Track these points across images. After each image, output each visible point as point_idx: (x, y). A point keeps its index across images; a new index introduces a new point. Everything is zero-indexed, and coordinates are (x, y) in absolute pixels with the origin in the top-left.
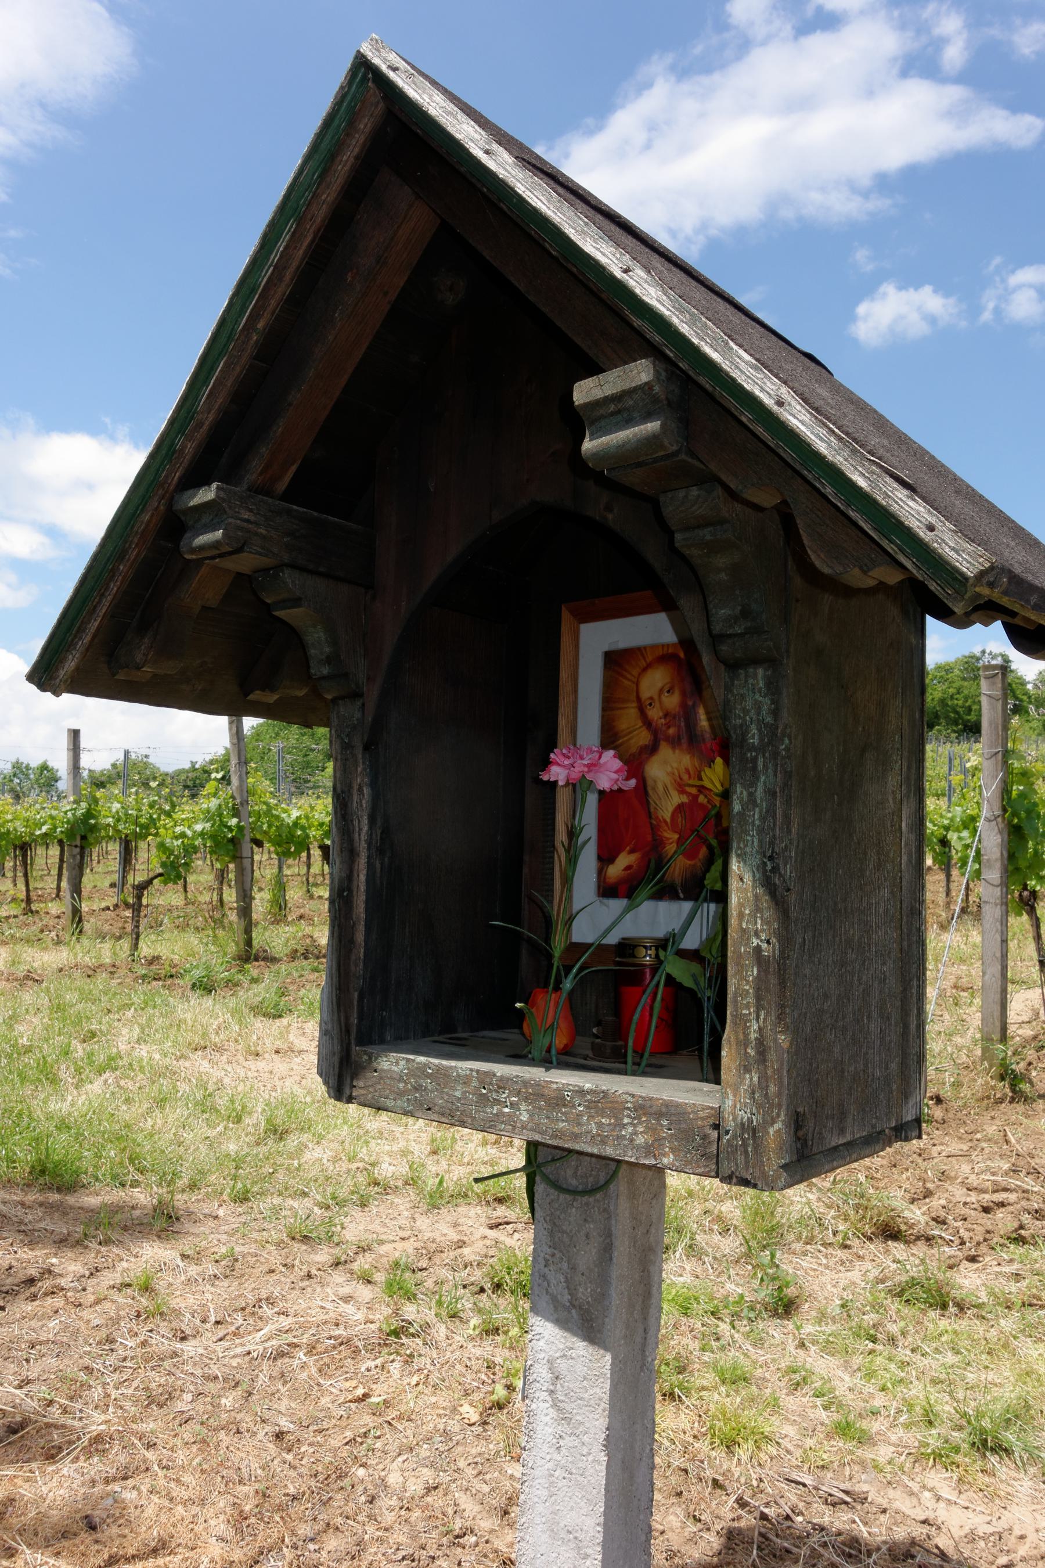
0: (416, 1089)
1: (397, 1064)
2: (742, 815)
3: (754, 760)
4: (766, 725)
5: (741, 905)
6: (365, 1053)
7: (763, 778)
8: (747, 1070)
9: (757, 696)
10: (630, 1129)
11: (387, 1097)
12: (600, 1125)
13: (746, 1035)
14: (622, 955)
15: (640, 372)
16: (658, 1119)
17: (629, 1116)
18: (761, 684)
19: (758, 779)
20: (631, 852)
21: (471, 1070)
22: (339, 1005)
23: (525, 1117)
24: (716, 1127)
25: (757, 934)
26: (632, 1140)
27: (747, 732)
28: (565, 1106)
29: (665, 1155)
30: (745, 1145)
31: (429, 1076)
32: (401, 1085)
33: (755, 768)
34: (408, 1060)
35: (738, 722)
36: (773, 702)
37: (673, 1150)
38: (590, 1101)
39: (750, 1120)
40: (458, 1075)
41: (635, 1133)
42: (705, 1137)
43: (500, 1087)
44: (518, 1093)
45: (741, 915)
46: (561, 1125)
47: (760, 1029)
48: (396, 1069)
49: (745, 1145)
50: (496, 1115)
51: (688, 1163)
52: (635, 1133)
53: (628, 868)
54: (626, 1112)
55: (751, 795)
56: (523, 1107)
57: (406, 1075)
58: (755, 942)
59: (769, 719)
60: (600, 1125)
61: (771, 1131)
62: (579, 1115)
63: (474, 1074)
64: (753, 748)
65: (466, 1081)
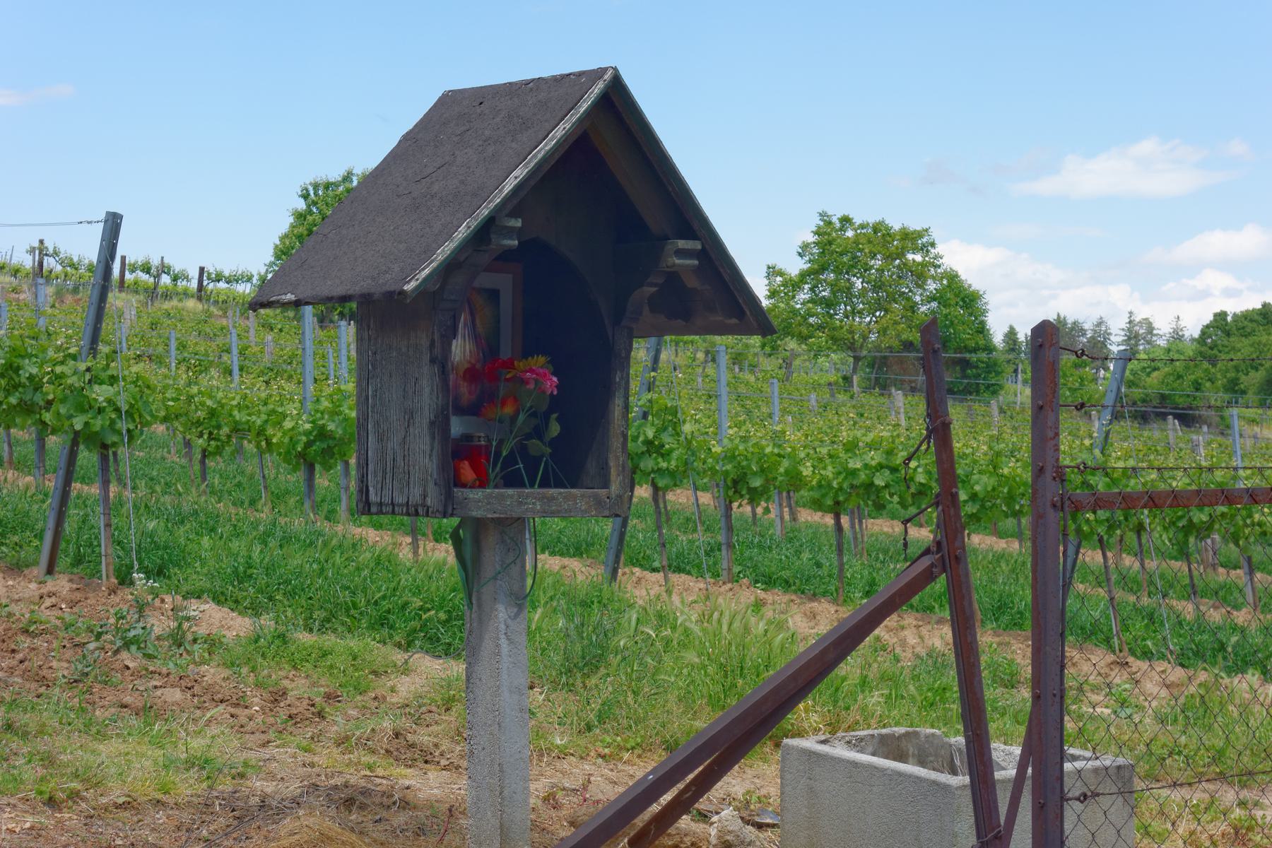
15: (697, 245)
65: (512, 497)
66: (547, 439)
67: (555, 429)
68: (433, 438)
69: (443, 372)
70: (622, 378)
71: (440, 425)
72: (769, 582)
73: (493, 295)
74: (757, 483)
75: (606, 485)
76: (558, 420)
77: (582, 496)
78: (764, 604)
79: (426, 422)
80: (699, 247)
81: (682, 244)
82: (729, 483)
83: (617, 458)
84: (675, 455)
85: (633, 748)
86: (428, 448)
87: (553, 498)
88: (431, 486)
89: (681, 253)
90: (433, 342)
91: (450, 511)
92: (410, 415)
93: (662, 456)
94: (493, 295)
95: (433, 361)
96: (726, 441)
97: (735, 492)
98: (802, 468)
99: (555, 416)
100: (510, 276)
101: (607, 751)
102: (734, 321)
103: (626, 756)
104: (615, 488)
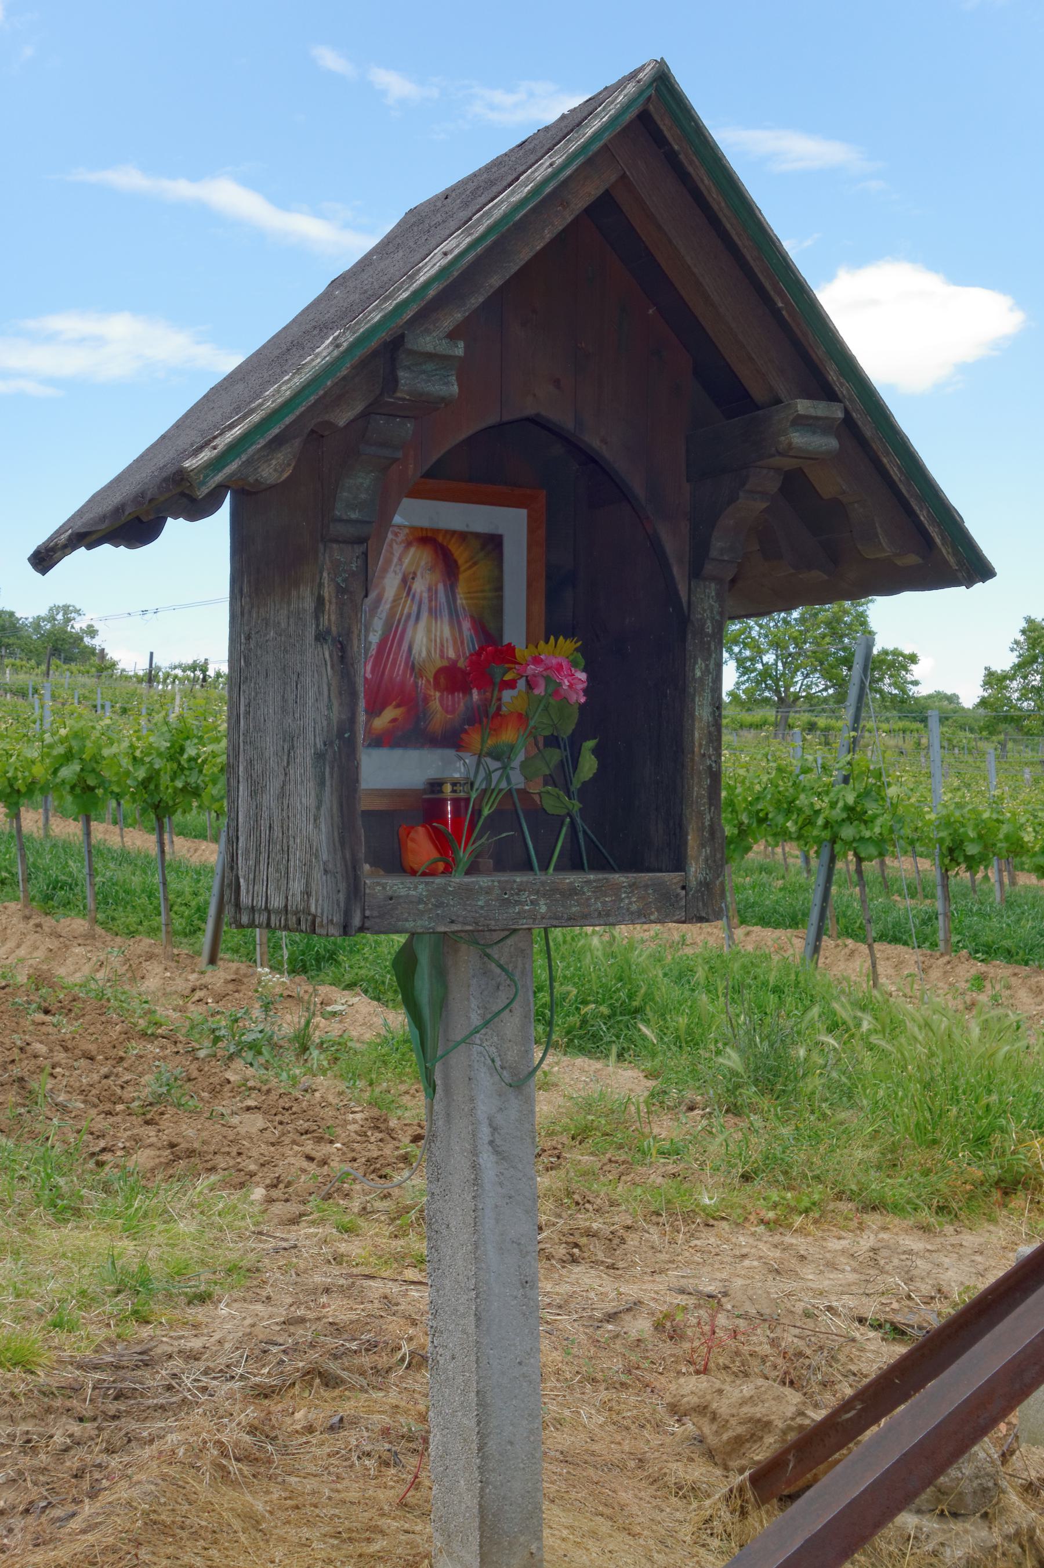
0: (437, 907)
1: (416, 888)
2: (701, 679)
3: (709, 643)
4: (717, 621)
5: (701, 739)
6: (378, 884)
7: (714, 655)
8: (703, 846)
9: (711, 601)
10: (627, 901)
11: (407, 920)
12: (604, 903)
13: (703, 824)
14: (433, 792)
16: (646, 891)
17: (625, 892)
18: (713, 594)
19: (711, 655)
20: (398, 706)
21: (493, 881)
22: (342, 844)
23: (543, 909)
24: (684, 888)
25: (710, 758)
26: (628, 909)
27: (705, 623)
28: (576, 894)
29: (652, 913)
30: (703, 895)
31: (450, 893)
32: (421, 907)
33: (709, 649)
34: (427, 883)
35: (699, 616)
36: (720, 606)
37: (658, 910)
38: (597, 887)
39: (705, 878)
40: (481, 887)
41: (631, 903)
42: (678, 895)
43: (520, 890)
44: (537, 892)
45: (700, 745)
46: (574, 909)
47: (711, 818)
48: (414, 893)
49: (703, 895)
50: (519, 913)
51: (667, 916)
52: (631, 903)
53: (394, 720)
54: (623, 890)
55: (707, 666)
56: (542, 902)
57: (426, 896)
58: (708, 762)
59: (718, 617)
60: (604, 903)
61: (718, 883)
62: (589, 899)
63: (496, 884)
64: (707, 635)
65: (488, 891)
66: (576, 785)
67: (588, 765)
68: (322, 784)
69: (342, 659)
70: (706, 671)
71: (340, 758)
72: (988, 951)
73: (493, 544)
74: (972, 849)
75: (679, 865)
76: (596, 752)
77: (633, 886)
78: (985, 978)
79: (310, 752)
80: (840, 415)
81: (803, 406)
82: (944, 851)
83: (701, 814)
84: (879, 821)
85: (807, 1211)
86: (311, 801)
87: (573, 892)
88: (317, 874)
89: (803, 422)
90: (320, 601)
91: (357, 921)
92: (290, 739)
93: (865, 822)
94: (493, 544)
95: (321, 637)
96: (939, 808)
97: (952, 860)
98: (1022, 834)
99: (590, 744)
100: (523, 512)
101: (771, 1215)
102: (912, 559)
103: (798, 1221)
104: (695, 870)
